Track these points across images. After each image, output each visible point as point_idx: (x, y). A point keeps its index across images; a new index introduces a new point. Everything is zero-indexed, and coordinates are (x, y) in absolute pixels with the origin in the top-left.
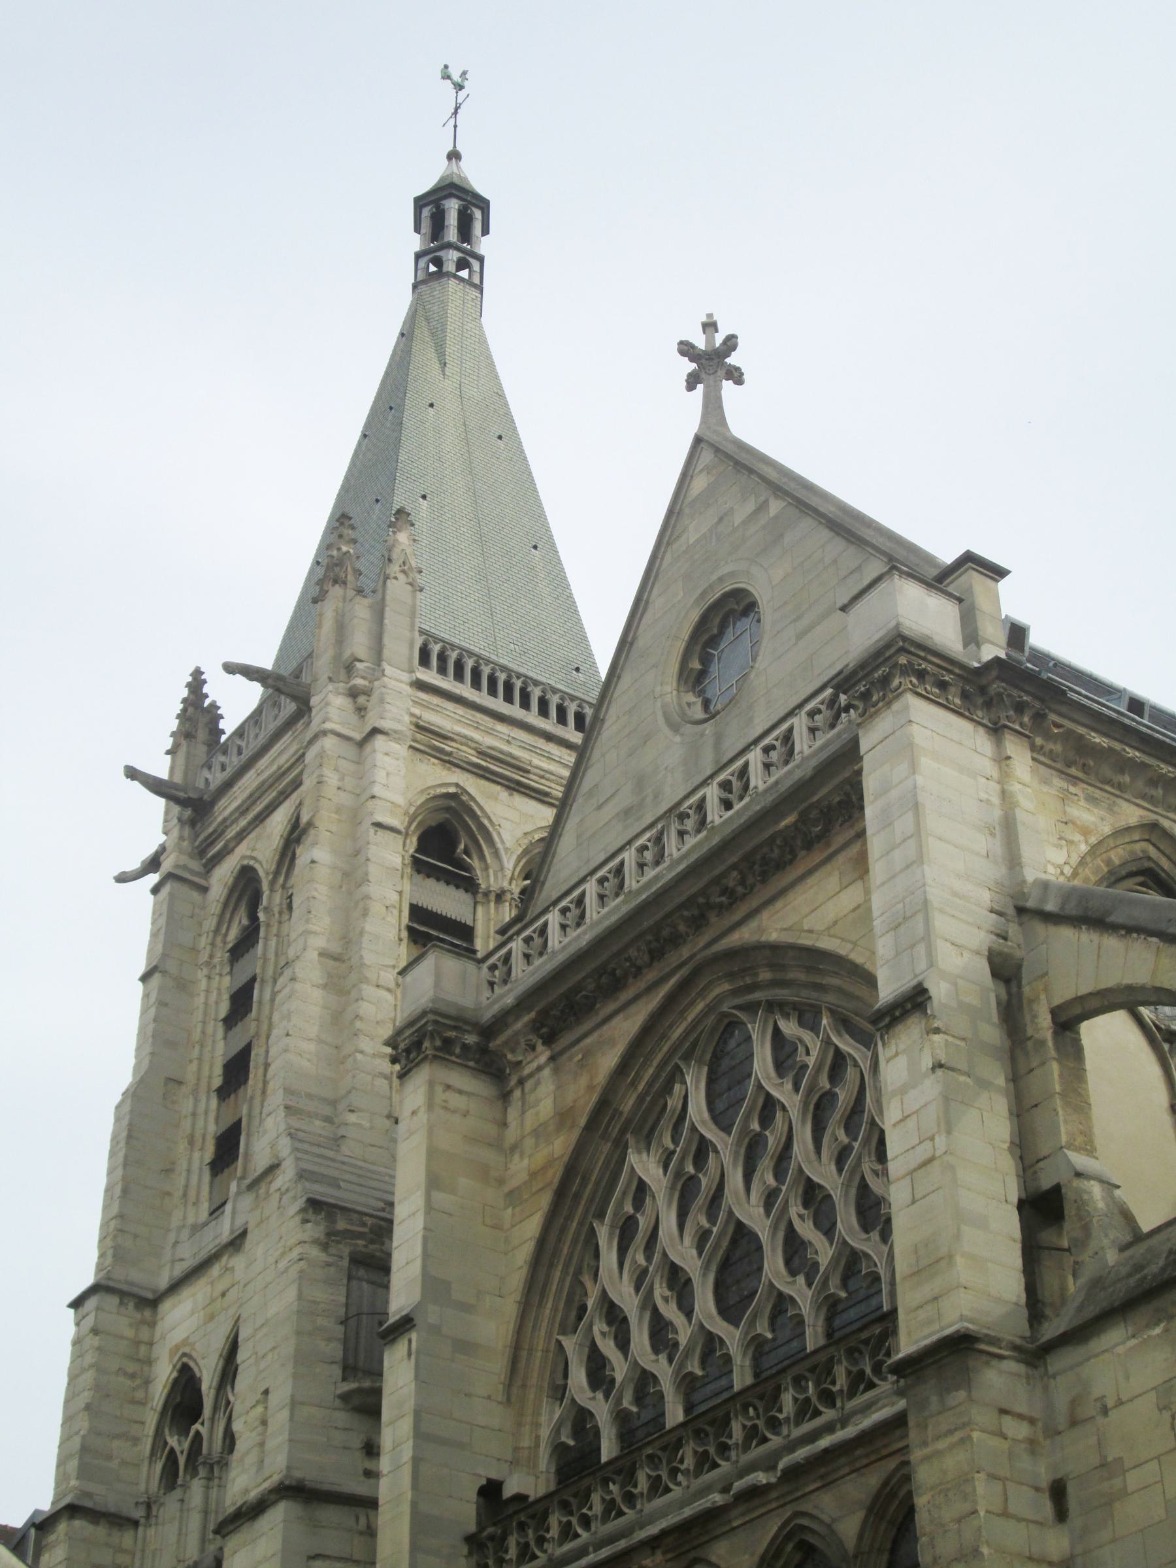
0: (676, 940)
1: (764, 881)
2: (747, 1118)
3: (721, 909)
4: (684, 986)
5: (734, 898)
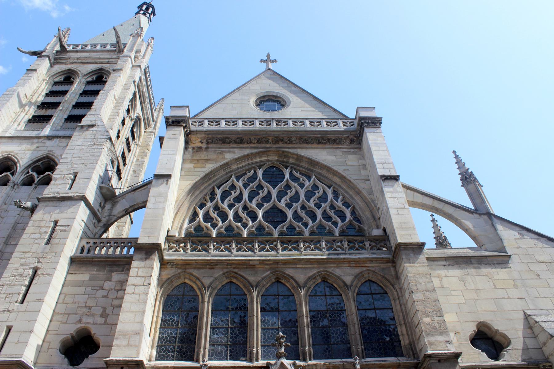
0: (267, 142)
1: (300, 144)
2: (282, 185)
3: (286, 143)
4: (265, 152)
5: (291, 142)
